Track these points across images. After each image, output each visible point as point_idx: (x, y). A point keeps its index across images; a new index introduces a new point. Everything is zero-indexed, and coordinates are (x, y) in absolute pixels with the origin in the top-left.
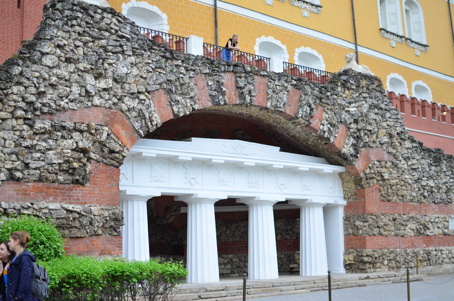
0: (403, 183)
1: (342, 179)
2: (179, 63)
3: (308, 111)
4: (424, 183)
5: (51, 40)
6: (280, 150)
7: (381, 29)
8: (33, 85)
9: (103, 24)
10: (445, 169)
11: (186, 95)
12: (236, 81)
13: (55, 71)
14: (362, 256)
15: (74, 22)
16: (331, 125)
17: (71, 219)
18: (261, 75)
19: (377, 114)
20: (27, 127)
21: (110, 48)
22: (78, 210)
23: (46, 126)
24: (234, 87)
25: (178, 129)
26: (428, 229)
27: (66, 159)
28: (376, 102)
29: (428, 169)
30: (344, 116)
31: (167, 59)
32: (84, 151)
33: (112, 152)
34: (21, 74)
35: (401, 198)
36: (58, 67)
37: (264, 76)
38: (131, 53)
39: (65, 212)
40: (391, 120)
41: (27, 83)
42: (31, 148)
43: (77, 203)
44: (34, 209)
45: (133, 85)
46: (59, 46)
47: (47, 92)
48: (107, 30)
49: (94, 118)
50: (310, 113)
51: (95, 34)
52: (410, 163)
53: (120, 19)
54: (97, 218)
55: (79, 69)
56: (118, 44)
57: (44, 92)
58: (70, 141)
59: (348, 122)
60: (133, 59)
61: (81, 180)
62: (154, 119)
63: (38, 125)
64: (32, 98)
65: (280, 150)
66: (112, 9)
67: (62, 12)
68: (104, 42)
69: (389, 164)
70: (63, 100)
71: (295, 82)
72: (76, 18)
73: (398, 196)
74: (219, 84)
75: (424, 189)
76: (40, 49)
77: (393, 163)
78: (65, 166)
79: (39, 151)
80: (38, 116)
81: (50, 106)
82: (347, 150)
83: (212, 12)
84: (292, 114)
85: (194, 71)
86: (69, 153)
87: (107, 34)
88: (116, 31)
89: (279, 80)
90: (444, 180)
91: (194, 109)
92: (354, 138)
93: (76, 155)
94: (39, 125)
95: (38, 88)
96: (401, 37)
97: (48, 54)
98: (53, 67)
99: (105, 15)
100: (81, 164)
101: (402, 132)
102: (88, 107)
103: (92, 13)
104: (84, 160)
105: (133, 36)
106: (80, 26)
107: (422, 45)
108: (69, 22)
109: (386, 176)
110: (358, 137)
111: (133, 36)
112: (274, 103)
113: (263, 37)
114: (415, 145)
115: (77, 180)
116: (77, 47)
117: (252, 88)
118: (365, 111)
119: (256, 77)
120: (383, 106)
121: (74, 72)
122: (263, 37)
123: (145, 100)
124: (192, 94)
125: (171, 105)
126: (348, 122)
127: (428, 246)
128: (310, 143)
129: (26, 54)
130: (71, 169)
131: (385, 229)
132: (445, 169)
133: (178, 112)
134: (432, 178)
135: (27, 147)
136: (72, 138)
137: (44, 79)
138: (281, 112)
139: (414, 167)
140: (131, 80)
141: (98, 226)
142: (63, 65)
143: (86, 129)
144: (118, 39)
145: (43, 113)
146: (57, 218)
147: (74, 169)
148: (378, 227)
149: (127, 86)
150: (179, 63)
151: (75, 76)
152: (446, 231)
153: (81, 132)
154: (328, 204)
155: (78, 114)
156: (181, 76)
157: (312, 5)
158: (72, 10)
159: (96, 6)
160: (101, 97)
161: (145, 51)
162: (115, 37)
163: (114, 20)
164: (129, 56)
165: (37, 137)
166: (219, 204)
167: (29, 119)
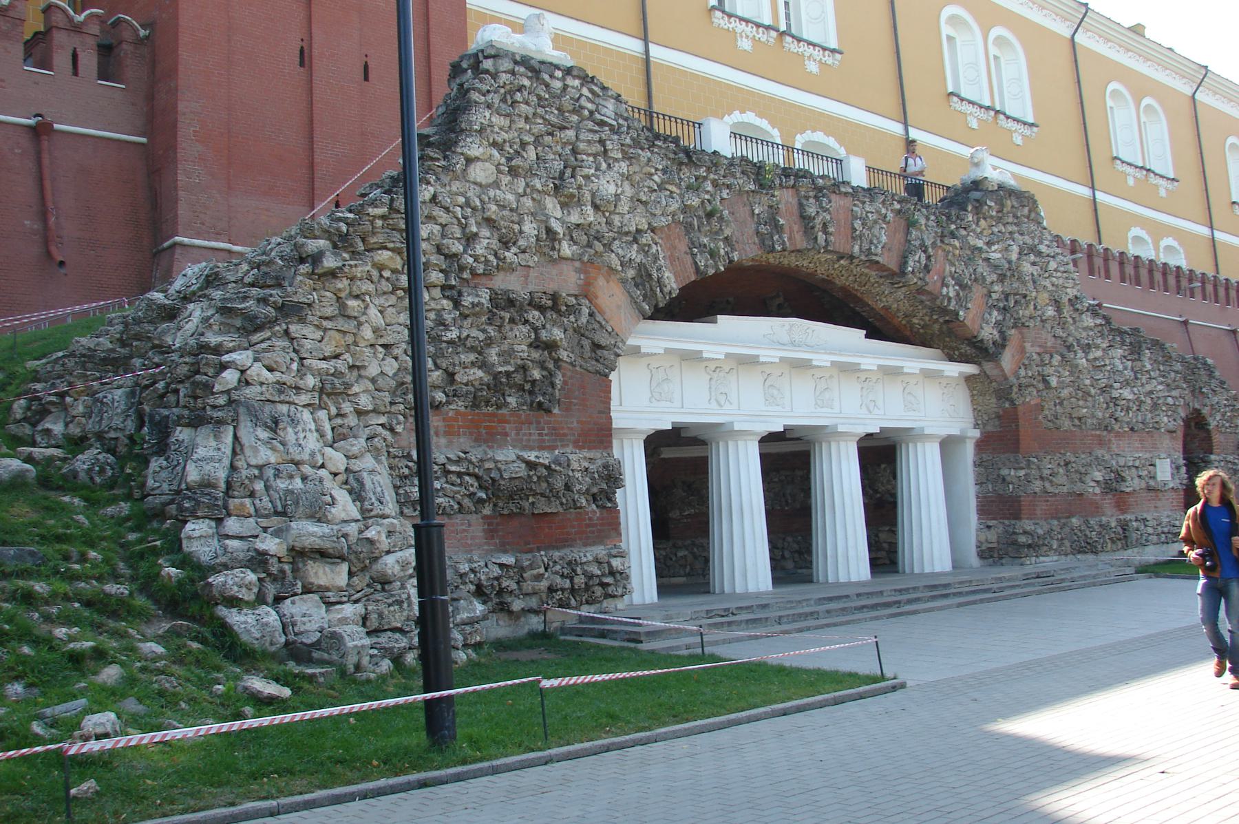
0: (1080, 394)
1: (971, 389)
2: (702, 172)
3: (923, 261)
4: (1115, 394)
5: (481, 131)
6: (867, 336)
7: (951, 94)
8: (455, 221)
9: (566, 102)
10: (1149, 367)
11: (717, 233)
12: (801, 205)
13: (492, 193)
14: (1014, 533)
15: (518, 96)
16: (961, 286)
17: (535, 479)
18: (840, 193)
19: (1034, 264)
20: (451, 303)
21: (582, 146)
22: (546, 462)
23: (483, 301)
24: (796, 218)
25: (697, 302)
26: (1123, 480)
27: (519, 362)
28: (1029, 241)
29: (1121, 368)
30: (982, 268)
31: (681, 164)
32: (551, 346)
33: (596, 346)
34: (434, 199)
35: (1076, 422)
36: (496, 185)
37: (846, 194)
38: (620, 156)
39: (523, 465)
40: (1059, 274)
41: (444, 217)
43: (541, 448)
44: (470, 462)
45: (627, 216)
46: (494, 144)
47: (481, 234)
48: (574, 111)
49: (566, 281)
50: (926, 266)
51: (554, 120)
52: (1091, 356)
53: (596, 89)
54: (578, 475)
55: (534, 189)
56: (597, 137)
57: (476, 234)
58: (525, 329)
59: (989, 280)
60: (624, 167)
61: (547, 404)
62: (667, 281)
63: (467, 300)
64: (457, 247)
65: (867, 336)
66: (580, 69)
67: (495, 76)
68: (571, 134)
69: (1057, 358)
70: (508, 249)
71: (897, 206)
72: (520, 89)
73: (1071, 418)
74: (774, 210)
75: (1116, 405)
76: (465, 150)
77: (1062, 356)
78: (518, 378)
79: (472, 349)
80: (466, 280)
81: (487, 262)
82: (988, 333)
83: (642, 67)
84: (893, 266)
85: (728, 187)
86: (522, 348)
87: (575, 118)
88: (591, 113)
89: (871, 201)
90: (1148, 388)
91: (731, 261)
92: (998, 310)
93: (536, 355)
94: (470, 299)
95: (464, 227)
96: (988, 108)
97: (477, 159)
98: (489, 185)
99: (571, 82)
100: (545, 373)
101: (1076, 297)
102: (553, 261)
103: (546, 77)
104: (551, 366)
105: (621, 121)
106: (527, 103)
107: (1025, 123)
108: (508, 97)
109: (1054, 382)
110: (1004, 308)
111: (621, 121)
112: (866, 246)
113: (737, 112)
114: (1099, 321)
115: (540, 404)
116: (523, 145)
117: (828, 217)
118: (1014, 257)
119: (833, 197)
120: (1043, 248)
121: (525, 194)
122: (737, 112)
123: (649, 245)
124: (727, 232)
125: (693, 255)
126: (989, 280)
127: (1124, 512)
128: (915, 321)
129: (438, 160)
130: (527, 382)
131: (1051, 482)
132: (1149, 367)
133: (706, 266)
134: (1128, 384)
135: (451, 342)
136: (526, 322)
137: (474, 209)
138: (877, 262)
139: (1098, 364)
140: (624, 207)
141: (579, 491)
142: (506, 179)
143: (550, 303)
144: (597, 128)
145: (474, 274)
146: (511, 479)
147: (534, 382)
148: (1042, 478)
149: (617, 220)
150: (702, 172)
151: (528, 203)
152: (1152, 483)
153: (542, 309)
154: (949, 436)
155: (533, 274)
156: (707, 197)
157: (825, 49)
158: (513, 73)
159: (551, 64)
160: (575, 243)
161: (642, 149)
162: (590, 125)
163: (585, 91)
164: (616, 160)
165: (467, 323)
166: (769, 439)
167: (452, 287)
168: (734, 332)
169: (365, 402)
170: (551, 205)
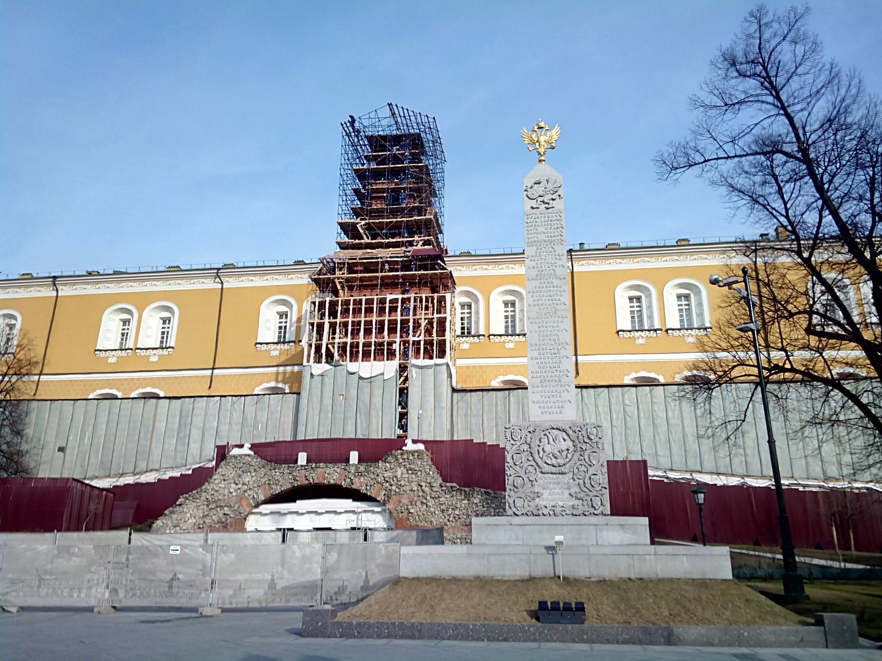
42: (206, 516)
60: (253, 474)
69: (419, 503)
86: (221, 515)
168: (302, 505)
169: (185, 528)
170: (233, 486)
